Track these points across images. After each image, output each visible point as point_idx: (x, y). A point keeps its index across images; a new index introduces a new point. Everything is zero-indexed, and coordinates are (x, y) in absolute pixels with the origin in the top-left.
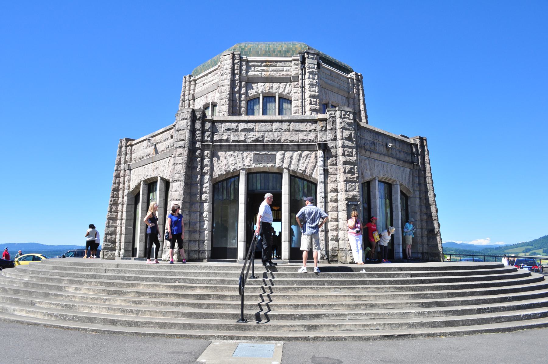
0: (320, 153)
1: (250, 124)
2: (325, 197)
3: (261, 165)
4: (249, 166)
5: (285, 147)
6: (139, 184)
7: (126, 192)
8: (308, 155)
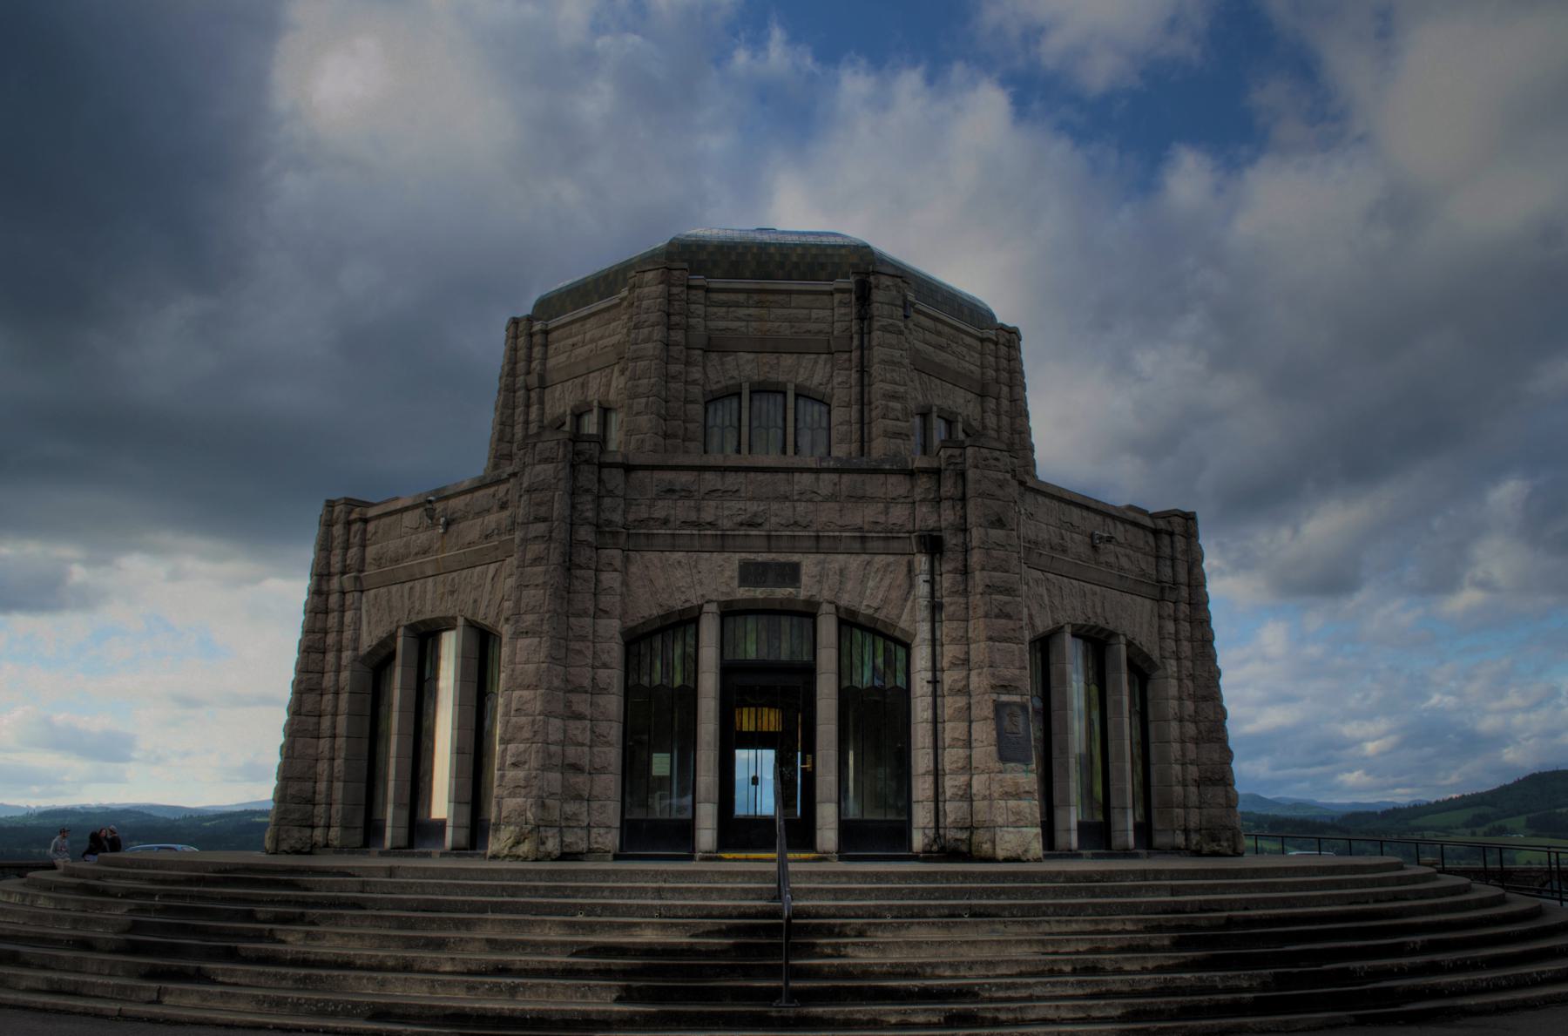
2: (934, 682)
3: (759, 593)
4: (728, 594)
5: (824, 544)
6: (392, 636)
7: (347, 655)
8: (888, 565)
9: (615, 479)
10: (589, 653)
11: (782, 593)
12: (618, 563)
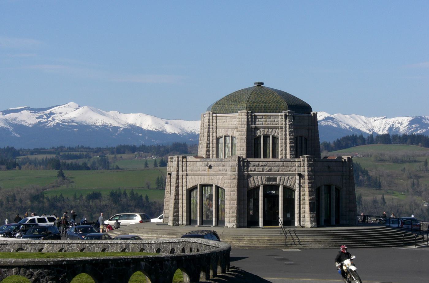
0: (298, 177)
2: (300, 198)
3: (271, 183)
7: (185, 188)
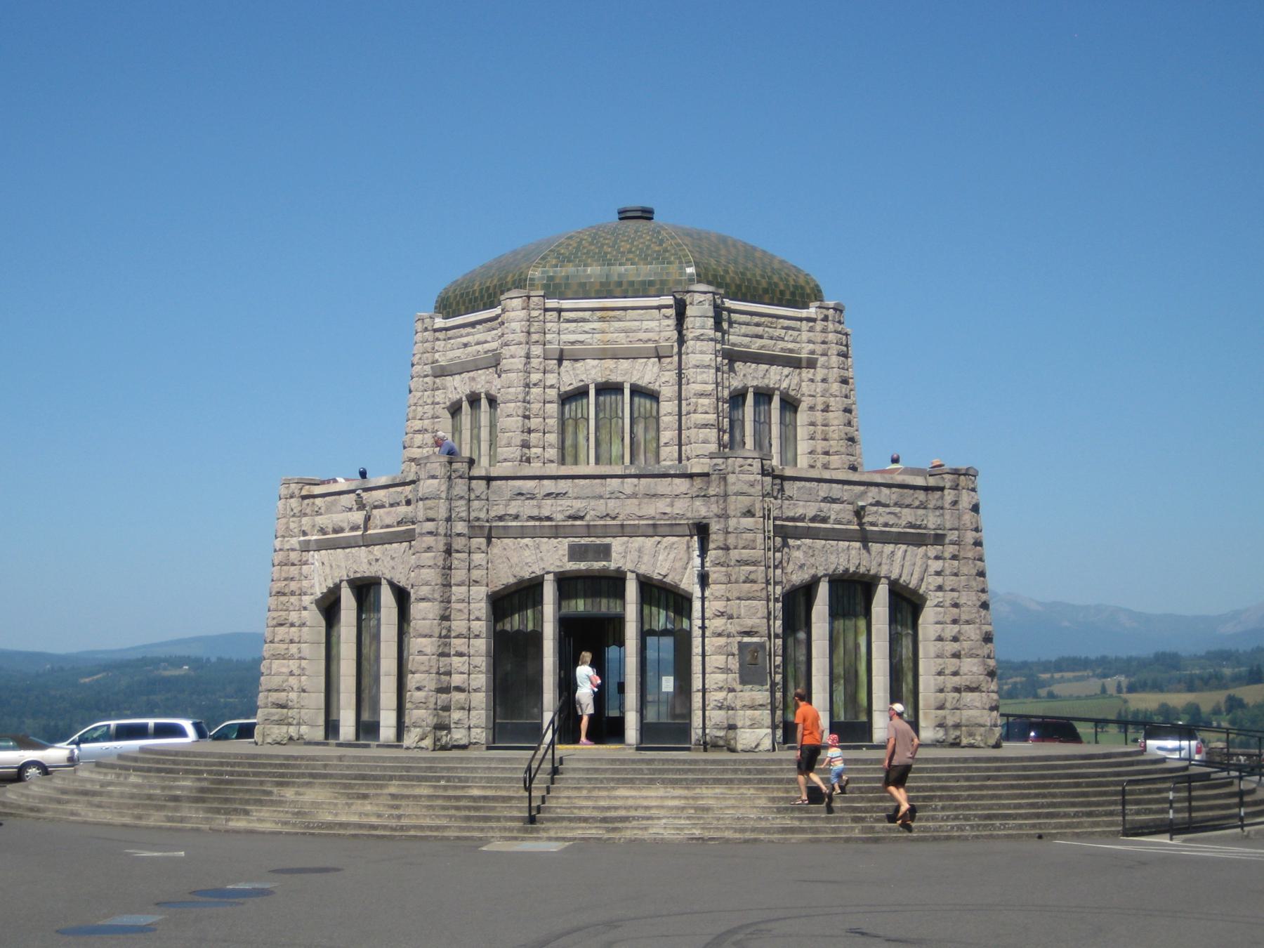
1: (562, 483)
2: (703, 628)
3: (582, 566)
9: (479, 486)
10: (466, 611)
11: (597, 565)
12: (484, 547)
